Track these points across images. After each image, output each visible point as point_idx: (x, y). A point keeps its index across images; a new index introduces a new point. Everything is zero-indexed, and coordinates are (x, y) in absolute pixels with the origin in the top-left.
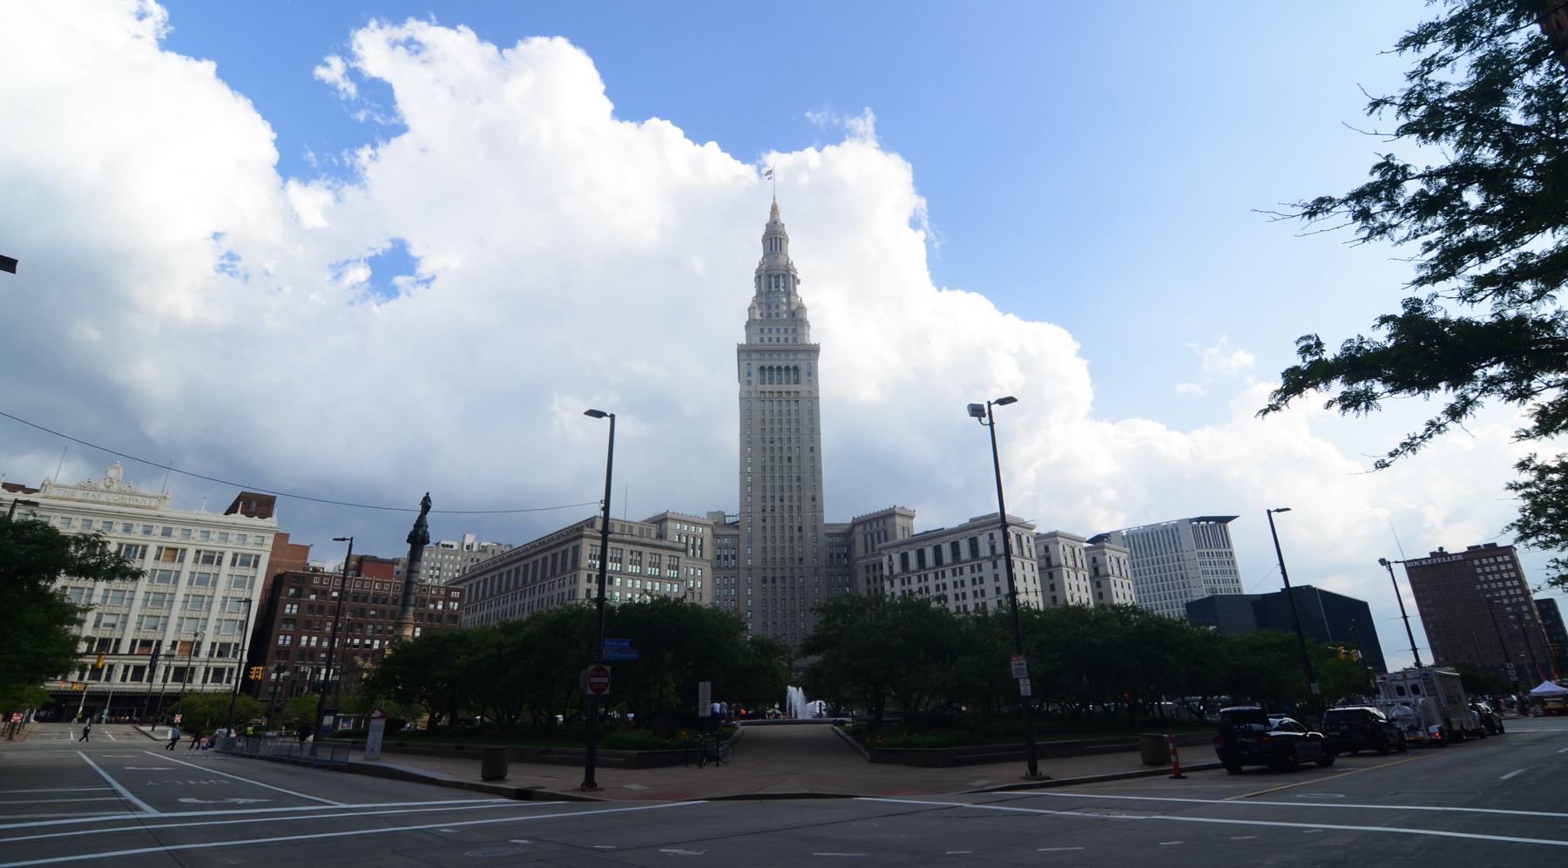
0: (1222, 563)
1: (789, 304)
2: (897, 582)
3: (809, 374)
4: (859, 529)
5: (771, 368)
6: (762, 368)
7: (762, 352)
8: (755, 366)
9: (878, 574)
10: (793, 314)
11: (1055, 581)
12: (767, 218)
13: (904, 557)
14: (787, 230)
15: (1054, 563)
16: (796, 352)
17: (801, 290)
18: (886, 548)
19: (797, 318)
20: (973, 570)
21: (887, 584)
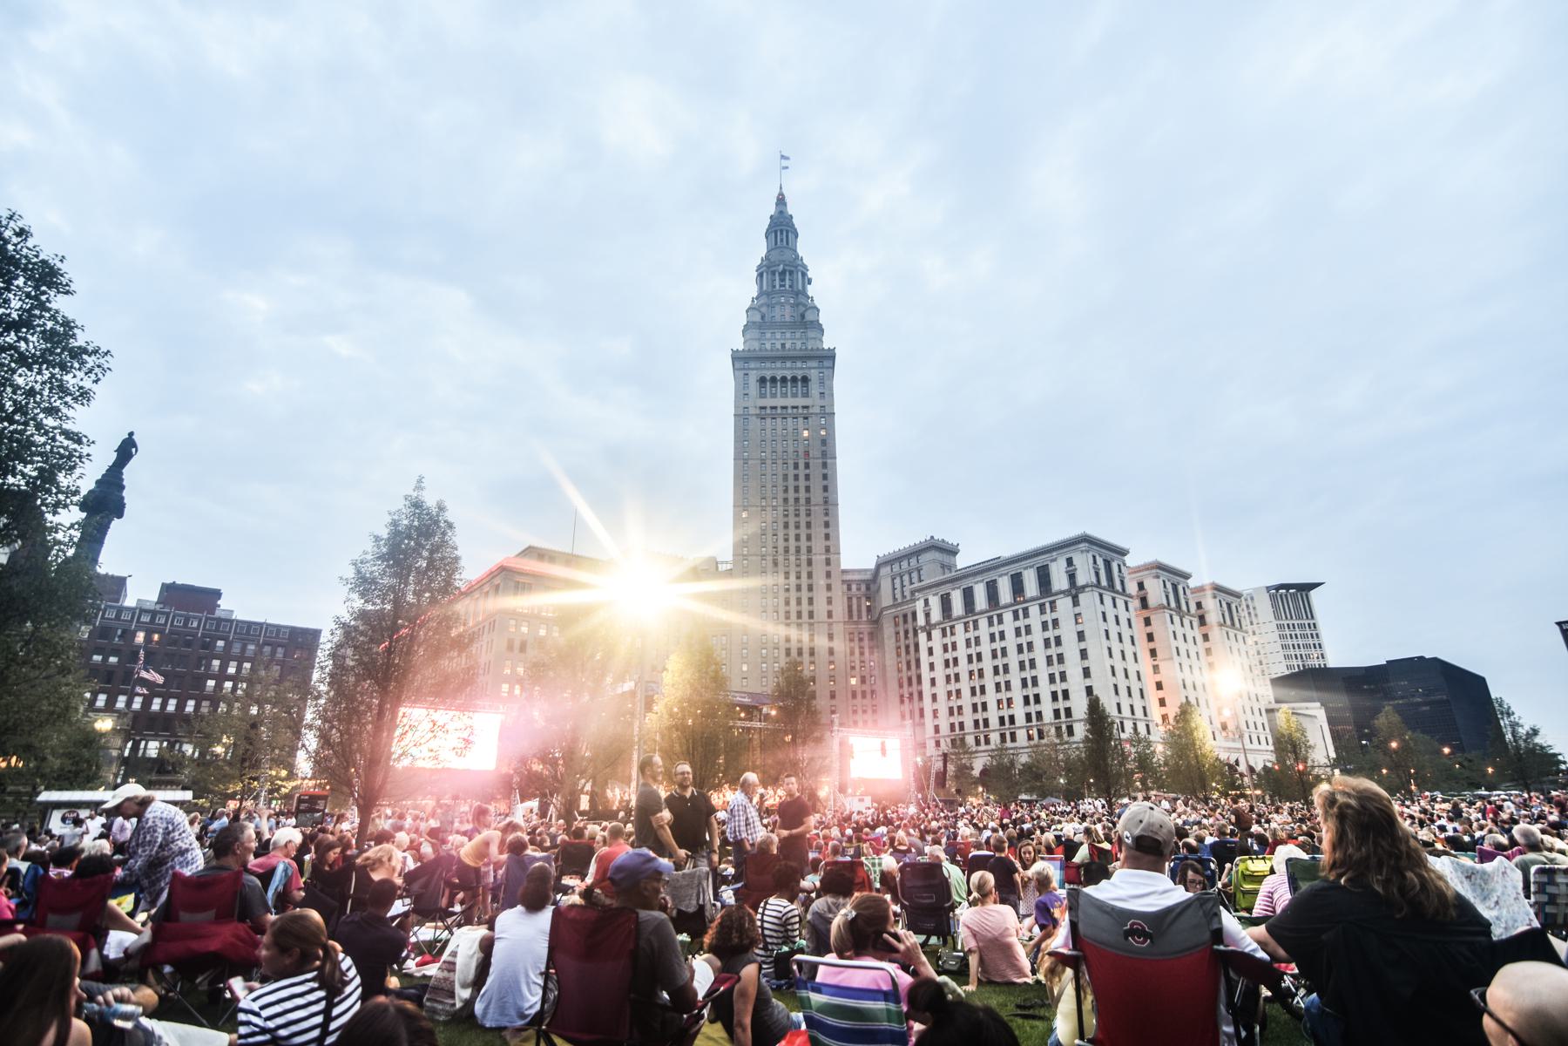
0: (1304, 636)
2: (936, 633)
3: (822, 382)
4: (885, 571)
5: (773, 380)
6: (762, 380)
8: (753, 377)
9: (910, 627)
11: (1155, 628)
12: (772, 210)
15: (1152, 602)
17: (811, 290)
18: (920, 590)
19: (806, 320)
20: (1043, 612)
21: (922, 637)
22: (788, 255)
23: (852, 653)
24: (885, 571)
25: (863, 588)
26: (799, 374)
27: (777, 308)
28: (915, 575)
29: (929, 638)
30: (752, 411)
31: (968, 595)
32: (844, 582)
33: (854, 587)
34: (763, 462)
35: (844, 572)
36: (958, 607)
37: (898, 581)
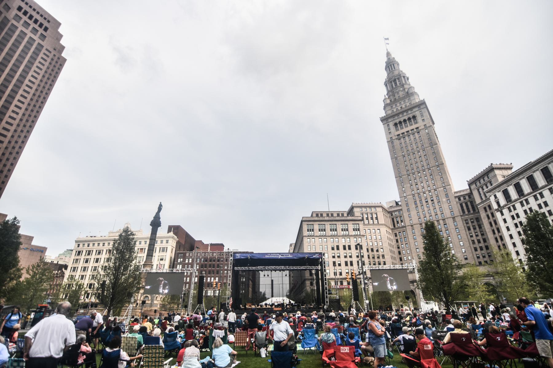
1: (404, 89)
2: (505, 211)
5: (400, 122)
6: (396, 125)
7: (393, 116)
8: (391, 124)
10: (407, 93)
12: (386, 59)
13: (506, 194)
14: (397, 59)
16: (411, 109)
21: (498, 214)
22: (396, 73)
23: (469, 229)
24: (473, 187)
25: (467, 197)
26: (411, 116)
27: (396, 95)
28: (489, 185)
29: (502, 214)
30: (394, 138)
31: (518, 187)
32: (455, 197)
33: (462, 198)
34: (404, 156)
35: (455, 193)
36: (514, 195)
37: (481, 190)
